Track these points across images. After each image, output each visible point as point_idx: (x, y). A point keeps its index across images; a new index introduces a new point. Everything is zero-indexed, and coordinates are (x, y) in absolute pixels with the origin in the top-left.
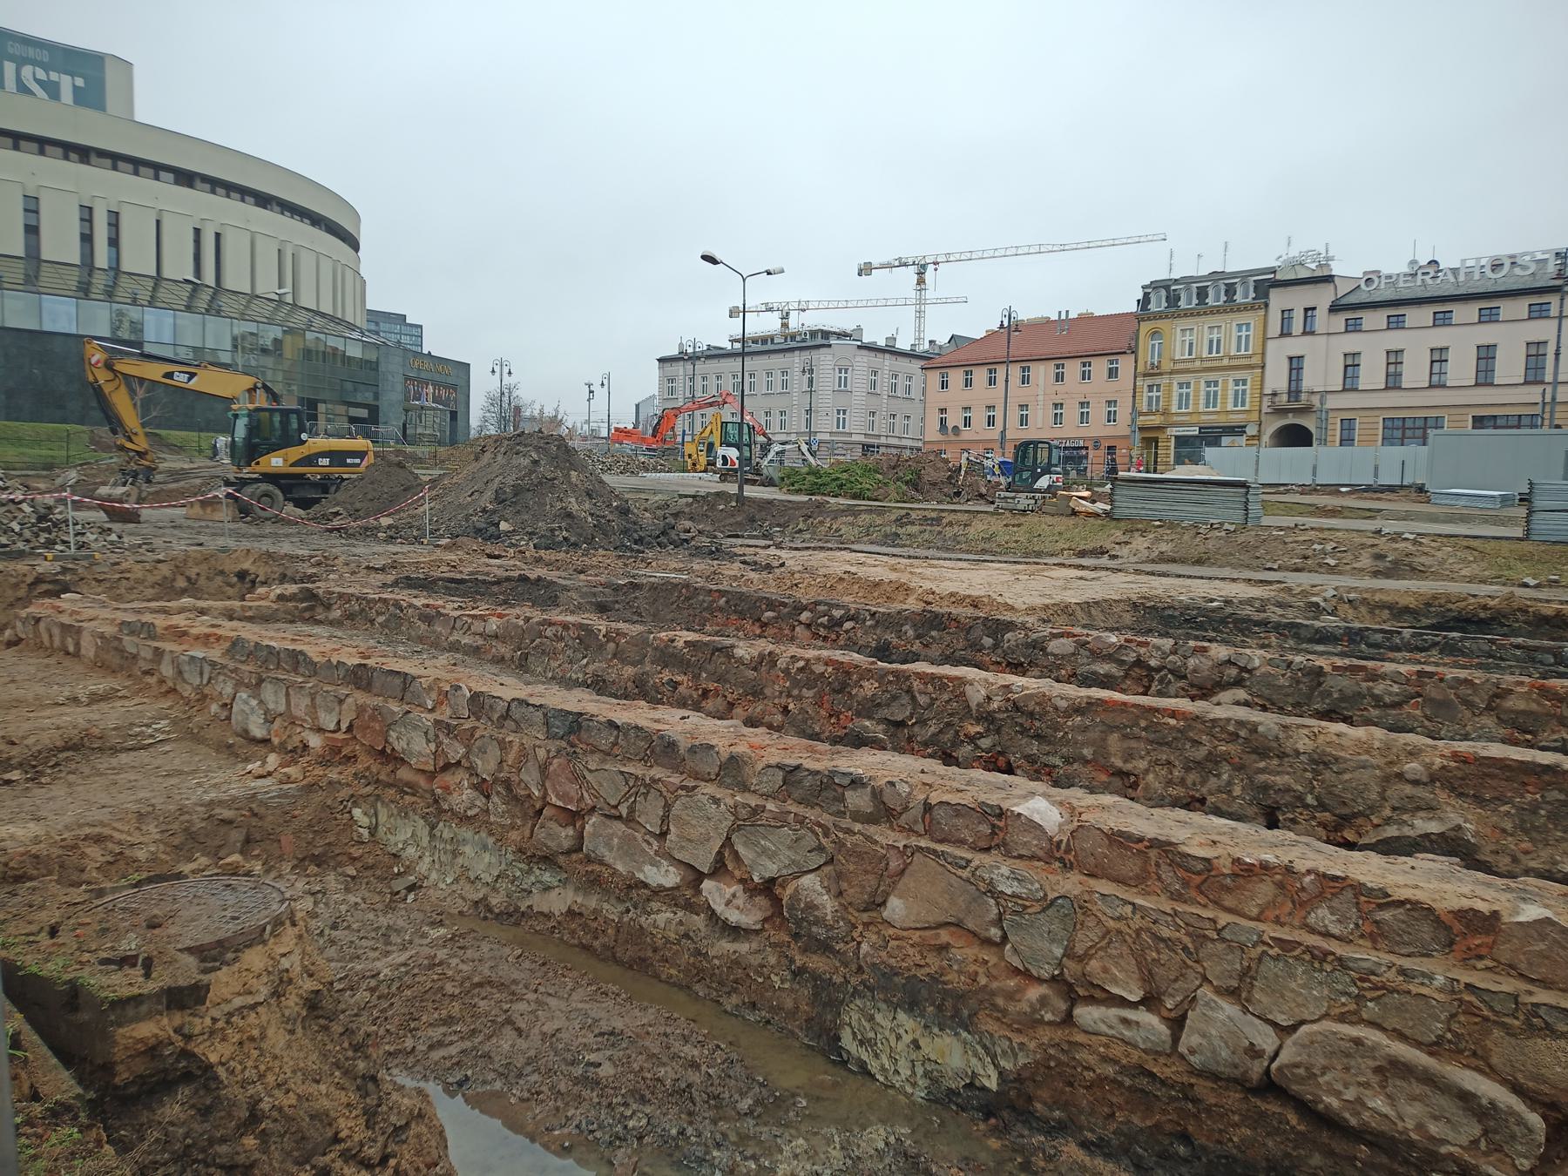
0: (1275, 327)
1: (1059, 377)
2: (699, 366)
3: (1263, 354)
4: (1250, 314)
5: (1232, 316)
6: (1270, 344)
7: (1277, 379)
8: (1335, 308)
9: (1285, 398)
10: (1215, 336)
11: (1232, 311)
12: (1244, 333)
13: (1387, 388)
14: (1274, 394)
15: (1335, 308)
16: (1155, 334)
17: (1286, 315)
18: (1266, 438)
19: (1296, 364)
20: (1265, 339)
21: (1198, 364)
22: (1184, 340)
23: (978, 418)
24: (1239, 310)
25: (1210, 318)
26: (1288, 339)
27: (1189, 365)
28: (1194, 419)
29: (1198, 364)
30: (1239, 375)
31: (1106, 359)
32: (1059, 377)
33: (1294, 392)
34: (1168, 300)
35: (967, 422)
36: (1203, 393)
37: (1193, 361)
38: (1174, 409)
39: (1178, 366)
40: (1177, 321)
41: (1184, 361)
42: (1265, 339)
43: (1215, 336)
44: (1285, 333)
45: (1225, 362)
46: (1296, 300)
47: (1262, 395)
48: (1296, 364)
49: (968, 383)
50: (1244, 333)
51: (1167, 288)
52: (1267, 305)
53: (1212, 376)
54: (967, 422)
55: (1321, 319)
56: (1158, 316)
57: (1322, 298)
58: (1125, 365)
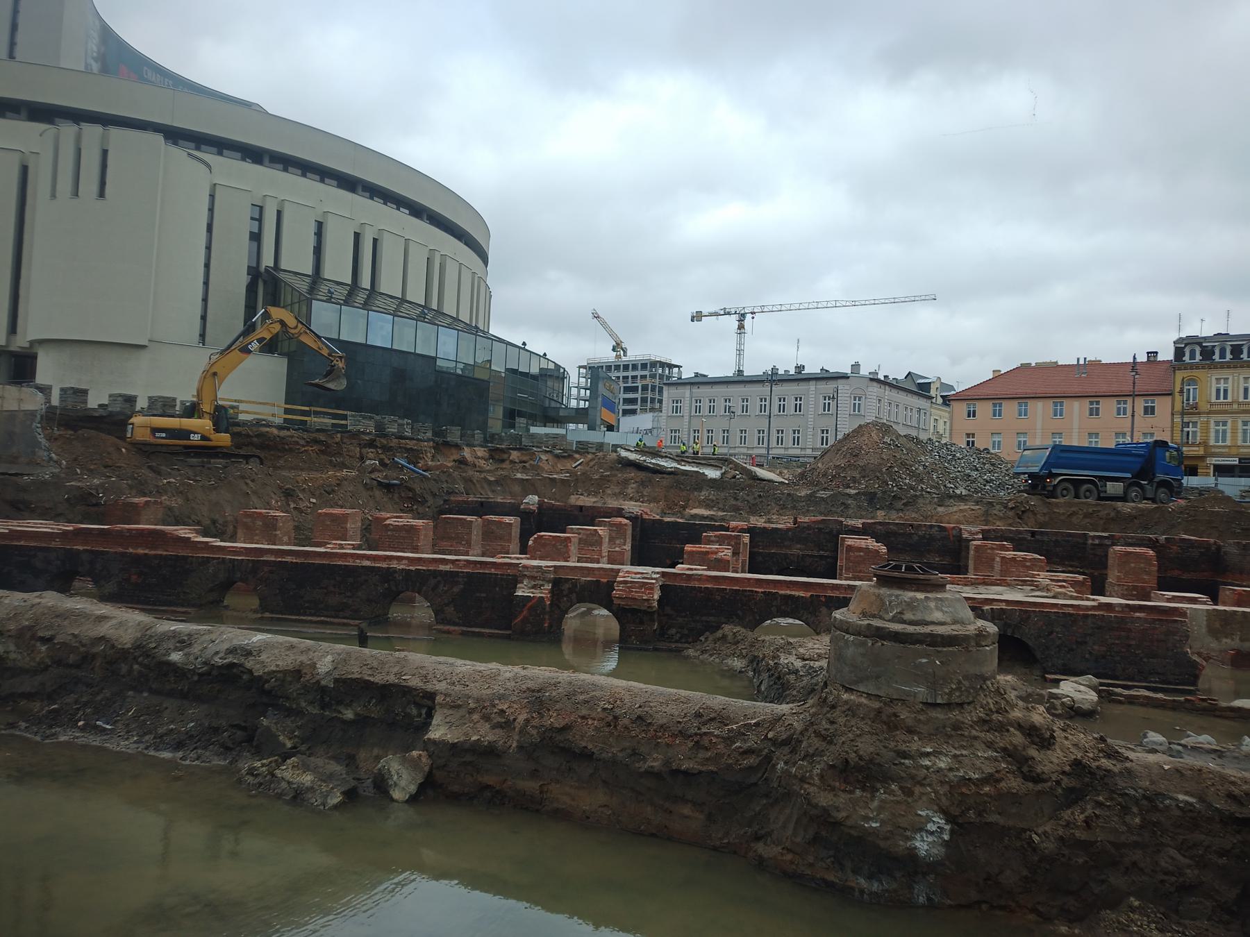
1: (1094, 412)
21: (1235, 406)
22: (1211, 385)
25: (1219, 371)
27: (1227, 408)
28: (1234, 451)
29: (1235, 406)
31: (1114, 400)
32: (1094, 412)
34: (1199, 354)
36: (1240, 431)
37: (1231, 404)
38: (1212, 443)
39: (1215, 408)
41: (1220, 404)
43: (1222, 386)
51: (1200, 344)
56: (1192, 367)
58: (1163, 406)
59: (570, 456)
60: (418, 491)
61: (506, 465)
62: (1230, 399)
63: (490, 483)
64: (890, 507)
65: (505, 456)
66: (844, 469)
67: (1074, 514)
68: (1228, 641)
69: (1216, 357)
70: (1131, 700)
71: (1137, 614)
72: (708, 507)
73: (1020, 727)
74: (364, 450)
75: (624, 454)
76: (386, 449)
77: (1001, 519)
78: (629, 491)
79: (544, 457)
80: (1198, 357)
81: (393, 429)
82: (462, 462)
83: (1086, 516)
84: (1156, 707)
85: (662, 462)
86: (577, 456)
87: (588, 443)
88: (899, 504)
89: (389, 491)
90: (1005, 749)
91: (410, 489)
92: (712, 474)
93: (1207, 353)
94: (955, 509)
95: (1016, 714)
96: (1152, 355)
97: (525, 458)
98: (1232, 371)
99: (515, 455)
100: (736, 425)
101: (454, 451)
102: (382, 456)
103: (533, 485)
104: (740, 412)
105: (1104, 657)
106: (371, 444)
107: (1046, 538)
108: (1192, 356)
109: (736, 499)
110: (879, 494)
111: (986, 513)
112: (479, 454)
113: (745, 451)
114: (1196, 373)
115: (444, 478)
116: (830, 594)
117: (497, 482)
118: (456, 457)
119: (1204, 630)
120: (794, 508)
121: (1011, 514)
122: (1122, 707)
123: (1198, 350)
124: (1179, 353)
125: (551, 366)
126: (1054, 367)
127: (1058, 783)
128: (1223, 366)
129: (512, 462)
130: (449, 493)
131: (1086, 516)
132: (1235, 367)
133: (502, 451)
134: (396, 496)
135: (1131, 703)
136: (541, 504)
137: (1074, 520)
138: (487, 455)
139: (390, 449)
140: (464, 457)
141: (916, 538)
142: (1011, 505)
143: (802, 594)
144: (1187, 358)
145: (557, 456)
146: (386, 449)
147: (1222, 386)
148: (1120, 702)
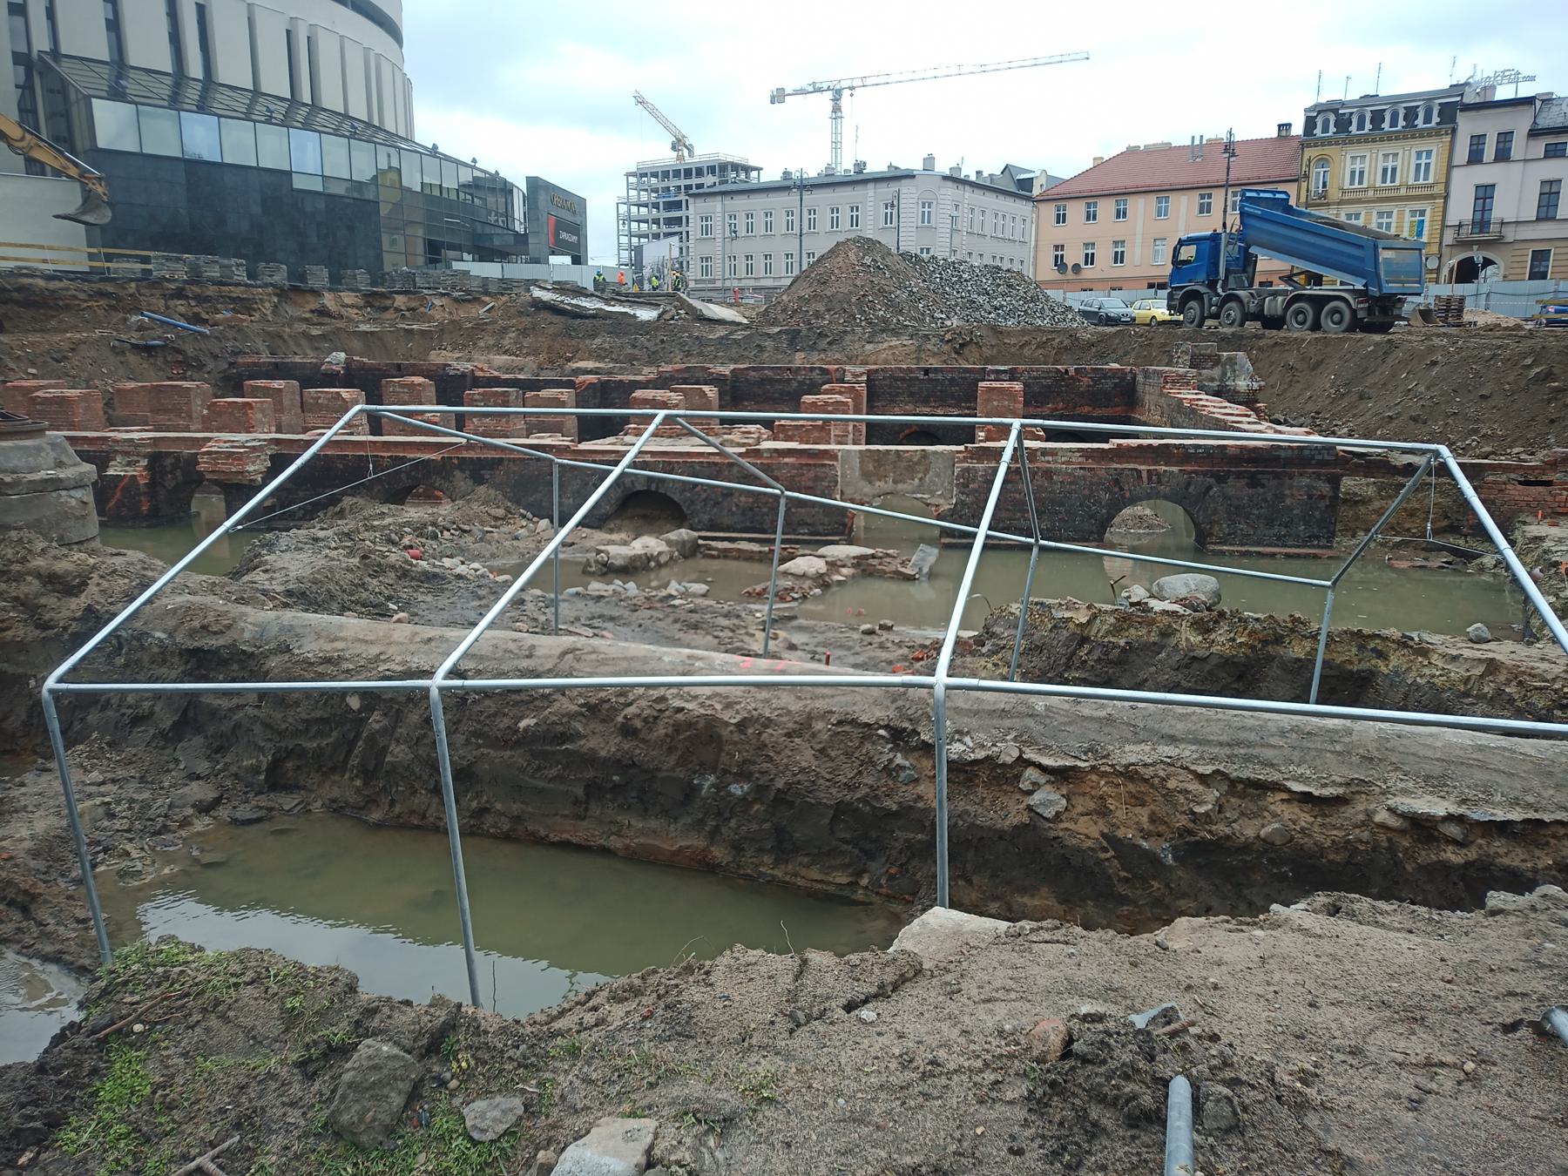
0: (1462, 153)
1: (1205, 209)
2: (807, 196)
3: (1447, 184)
4: (1434, 140)
5: (1411, 142)
6: (1456, 173)
7: (1462, 209)
8: (1534, 133)
9: (1466, 231)
10: (1390, 165)
11: (1413, 137)
12: (1423, 161)
13: (1538, 219)
14: (1460, 226)
15: (1534, 133)
16: (1323, 161)
17: (1478, 141)
18: (1445, 272)
19: (1485, 193)
20: (1450, 167)
21: (1371, 193)
23: (1104, 255)
24: (1421, 136)
26: (1477, 168)
27: (1360, 196)
30: (1418, 205)
33: (1481, 223)
35: (1090, 259)
37: (1365, 190)
40: (1349, 147)
41: (1354, 191)
42: (1450, 167)
43: (1358, 167)
44: (1475, 158)
45: (1403, 192)
46: (1490, 126)
47: (1444, 226)
48: (1485, 193)
49: (1091, 216)
50: (1423, 161)
51: (1335, 111)
52: (1454, 131)
53: (1385, 207)
54: (1090, 259)
55: (1518, 147)
57: (1521, 123)
59: (476, 299)
60: (190, 352)
61: (390, 315)
62: (1365, 185)
63: (311, 338)
64: (813, 348)
65: (388, 303)
66: (808, 301)
67: (1027, 344)
68: (882, 484)
69: (1353, 128)
70: (725, 554)
71: (786, 460)
72: (599, 358)
73: (39, 576)
74: (171, 303)
75: (537, 293)
76: (201, 299)
77: (934, 355)
78: (506, 342)
79: (437, 302)
80: (1332, 129)
81: (215, 273)
82: (323, 312)
83: (1040, 346)
84: (746, 559)
85: (586, 303)
86: (487, 299)
87: (511, 280)
88: (823, 344)
89: (150, 355)
90: (17, 599)
91: (179, 351)
92: (646, 314)
93: (1343, 124)
94: (885, 345)
95: (39, 562)
96: (1284, 127)
97: (413, 305)
98: (1370, 145)
99: (400, 301)
100: (740, 248)
101: (310, 298)
102: (197, 310)
103: (380, 339)
104: (744, 233)
105: (751, 509)
106: (179, 294)
107: (940, 377)
108: (1325, 130)
109: (634, 346)
110: (804, 332)
111: (919, 349)
112: (347, 301)
113: (752, 283)
114: (1327, 150)
115: (230, 334)
116: (465, 455)
117: (323, 337)
118: (313, 306)
119: (857, 474)
120: (700, 354)
121: (946, 348)
122: (716, 562)
123: (1332, 118)
124: (1310, 123)
125: (482, 175)
126: (1166, 150)
127: (65, 629)
128: (1360, 140)
129: (397, 310)
130: (234, 354)
131: (1040, 346)
132: (1374, 141)
133: (382, 295)
134: (160, 361)
135: (726, 557)
136: (348, 363)
137: (1026, 352)
138: (362, 303)
139: (207, 299)
140: (323, 305)
141: (795, 384)
142: (948, 337)
143: (432, 456)
144: (1318, 131)
145: (456, 300)
146: (201, 299)
147: (1358, 167)
148: (713, 557)
